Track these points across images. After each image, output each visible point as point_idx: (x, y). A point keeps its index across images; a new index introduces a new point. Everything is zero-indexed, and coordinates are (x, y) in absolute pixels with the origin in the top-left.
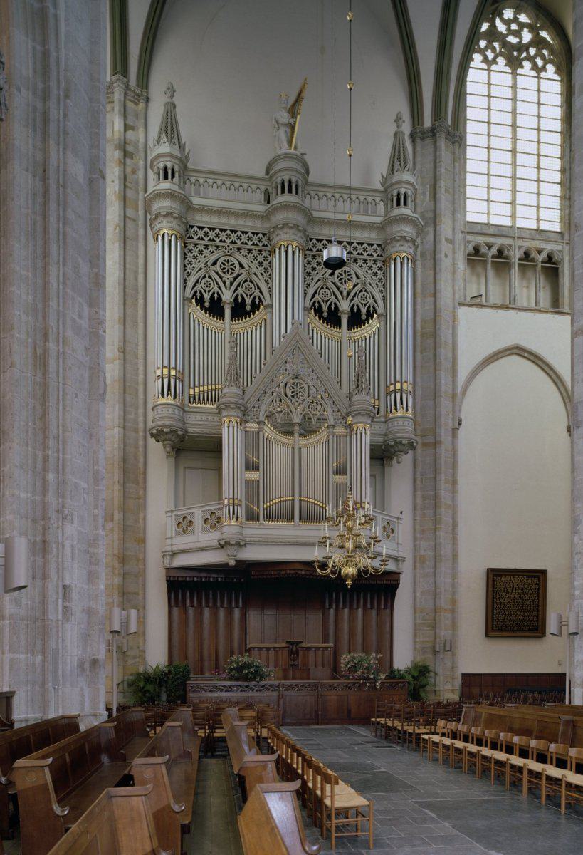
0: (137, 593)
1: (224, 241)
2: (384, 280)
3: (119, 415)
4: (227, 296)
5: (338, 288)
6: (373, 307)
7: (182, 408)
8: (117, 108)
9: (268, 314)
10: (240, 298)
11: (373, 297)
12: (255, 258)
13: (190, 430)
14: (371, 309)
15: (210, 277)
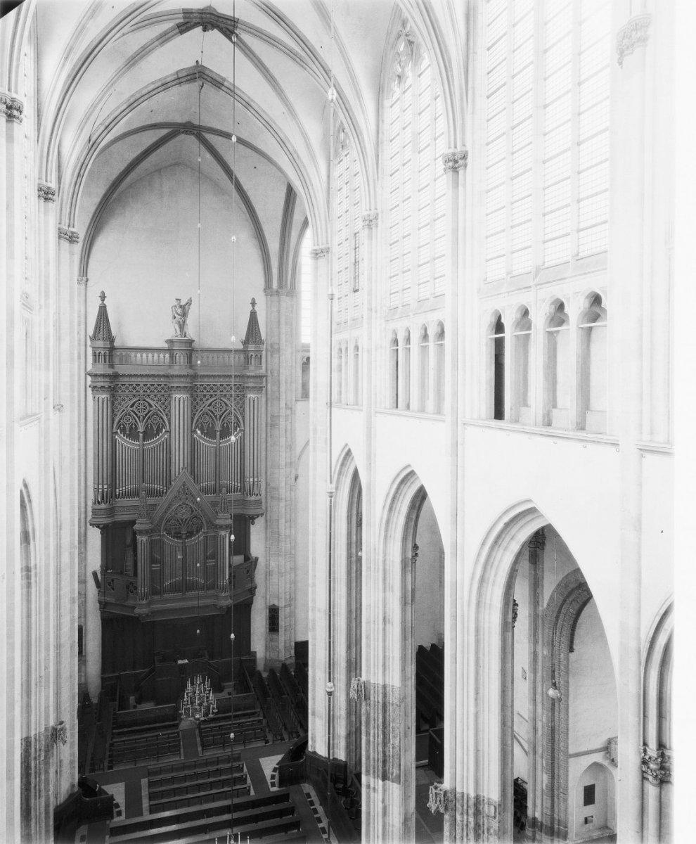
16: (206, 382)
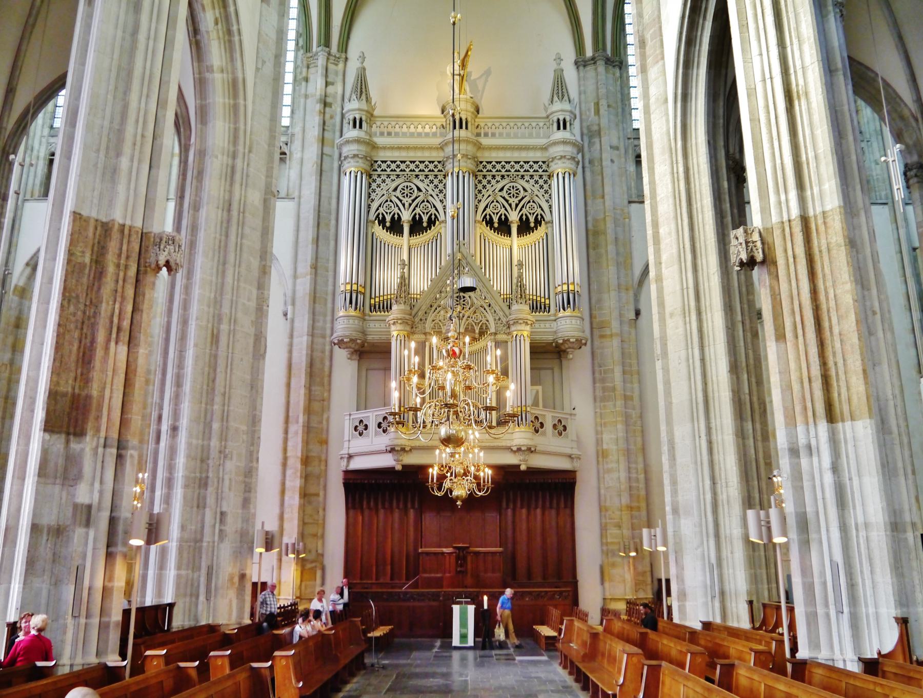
0: (317, 495)
1: (404, 171)
2: (549, 191)
3: (308, 325)
4: (406, 216)
5: (507, 201)
6: (541, 215)
7: (363, 318)
8: (320, 70)
9: (443, 229)
10: (417, 216)
11: (540, 207)
12: (432, 182)
13: (370, 338)
14: (539, 217)
15: (391, 201)
16: (494, 156)
